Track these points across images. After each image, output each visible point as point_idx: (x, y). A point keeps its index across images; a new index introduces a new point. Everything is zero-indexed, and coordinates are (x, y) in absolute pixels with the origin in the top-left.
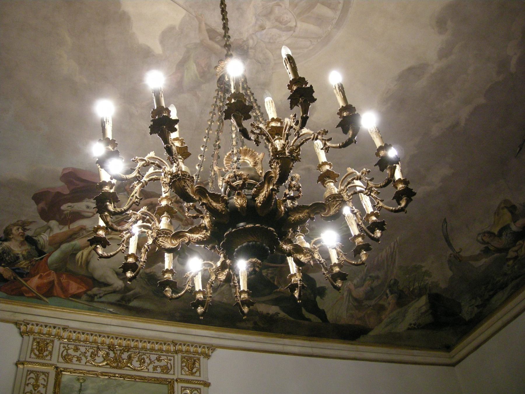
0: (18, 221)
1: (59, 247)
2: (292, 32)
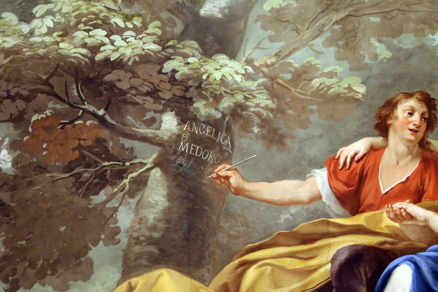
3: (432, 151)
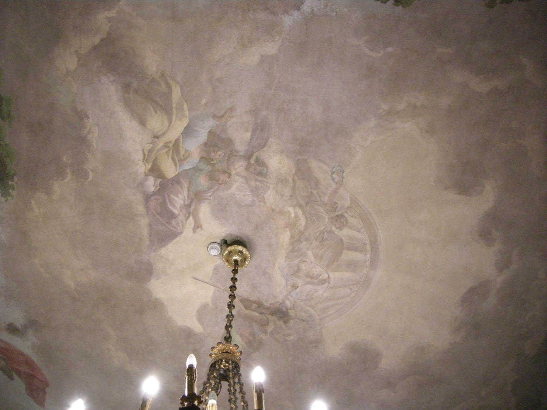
2: (326, 284)
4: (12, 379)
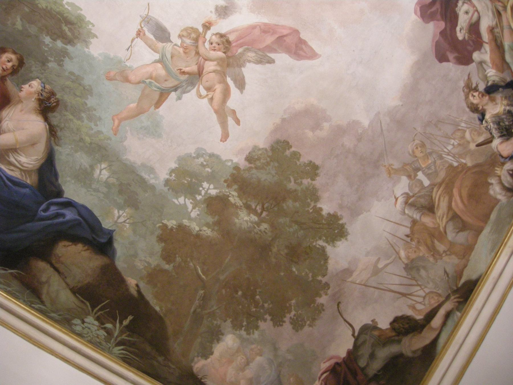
0: (463, 91)
1: (507, 64)
3: (4, 85)
4: (271, 61)
